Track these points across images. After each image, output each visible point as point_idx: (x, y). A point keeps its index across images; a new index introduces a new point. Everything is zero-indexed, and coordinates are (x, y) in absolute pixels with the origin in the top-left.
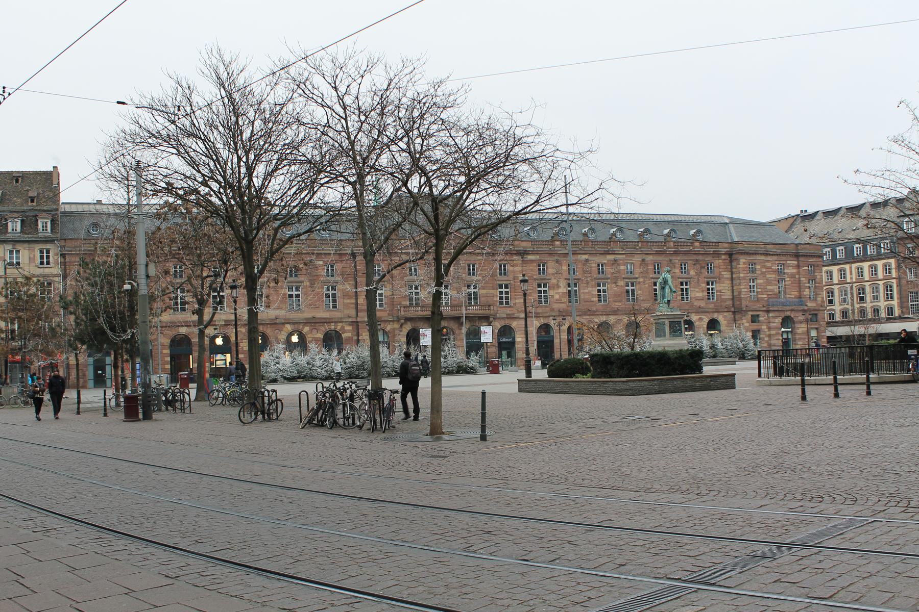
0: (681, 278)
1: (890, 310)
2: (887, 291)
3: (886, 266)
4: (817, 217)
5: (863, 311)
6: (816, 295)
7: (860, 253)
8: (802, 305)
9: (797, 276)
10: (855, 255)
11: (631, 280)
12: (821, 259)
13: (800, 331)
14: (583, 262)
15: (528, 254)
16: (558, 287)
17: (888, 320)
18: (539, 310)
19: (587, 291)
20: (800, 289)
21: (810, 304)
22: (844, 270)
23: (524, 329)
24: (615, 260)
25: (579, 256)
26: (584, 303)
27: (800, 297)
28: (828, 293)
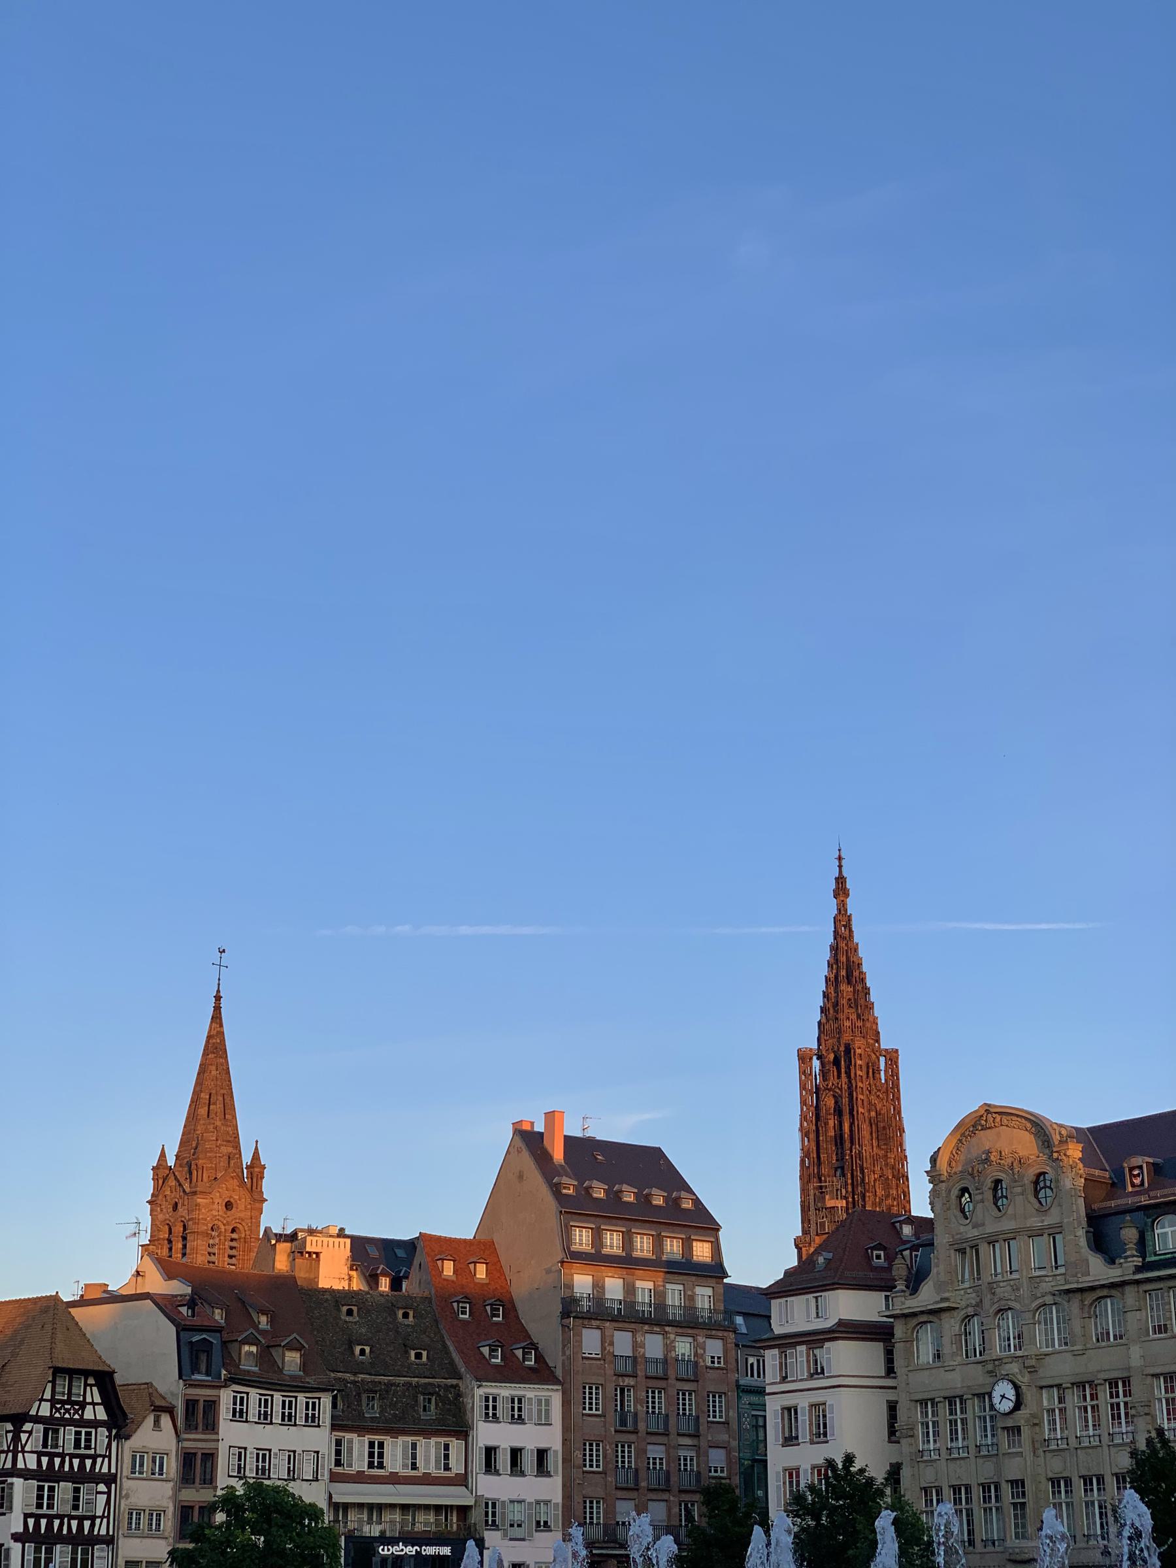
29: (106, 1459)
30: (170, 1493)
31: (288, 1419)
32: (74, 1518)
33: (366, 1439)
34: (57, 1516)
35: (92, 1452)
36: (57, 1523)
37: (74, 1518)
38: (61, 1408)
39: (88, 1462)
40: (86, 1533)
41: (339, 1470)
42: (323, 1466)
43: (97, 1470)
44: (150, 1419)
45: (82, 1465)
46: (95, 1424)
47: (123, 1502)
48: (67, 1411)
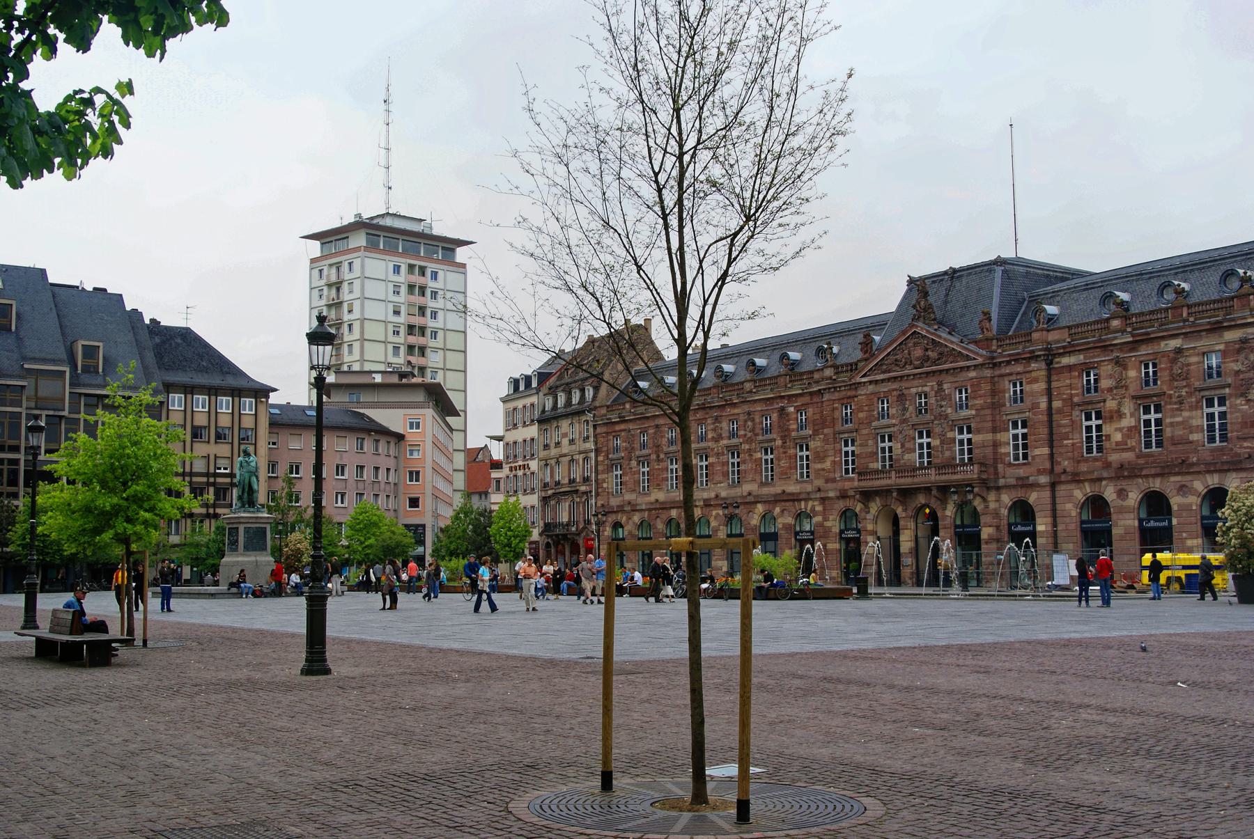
11: (1218, 392)
14: (1172, 355)
15: (1061, 355)
16: (1120, 415)
18: (1083, 467)
19: (1179, 419)
23: (1049, 507)
24: (1244, 341)
25: (1163, 344)
26: (1172, 448)
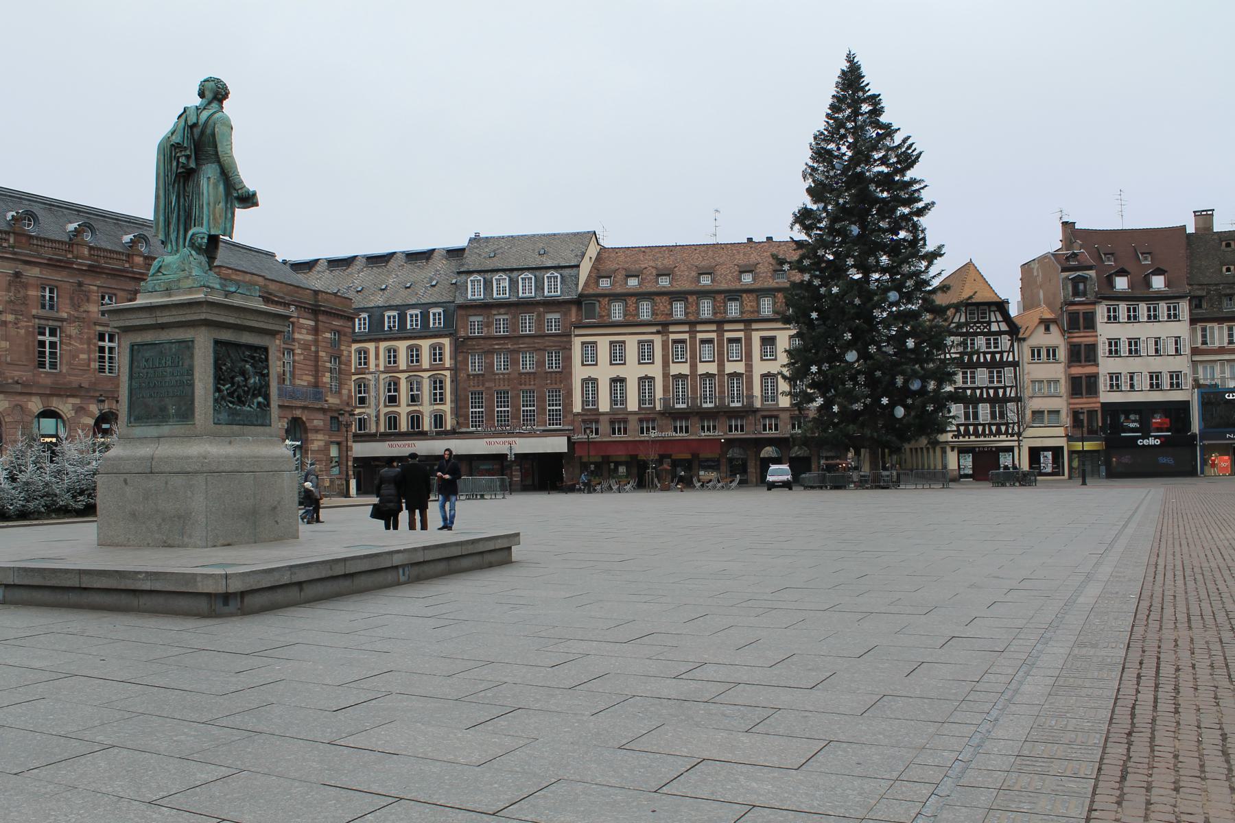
0: (101, 325)
1: (439, 419)
2: (435, 388)
3: (435, 349)
4: (318, 268)
5: (393, 421)
6: (341, 385)
7: (394, 326)
8: (319, 399)
9: (313, 348)
10: (386, 328)
12: (350, 324)
13: (315, 446)
17: (384, 437)
20: (317, 371)
21: (333, 400)
22: (366, 352)
27: (316, 385)
28: (360, 386)
29: (1011, 353)
30: (1063, 370)
31: (1153, 318)
32: (991, 388)
33: (1225, 326)
34: (978, 388)
35: (999, 350)
36: (978, 392)
37: (991, 388)
38: (973, 326)
39: (998, 356)
40: (1001, 396)
41: (1204, 347)
42: (1185, 345)
43: (1005, 360)
44: (1042, 328)
45: (993, 358)
46: (1000, 333)
47: (1026, 377)
48: (979, 327)
